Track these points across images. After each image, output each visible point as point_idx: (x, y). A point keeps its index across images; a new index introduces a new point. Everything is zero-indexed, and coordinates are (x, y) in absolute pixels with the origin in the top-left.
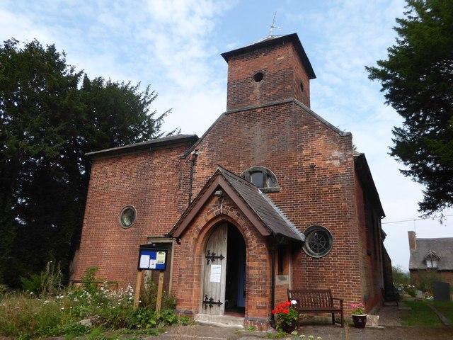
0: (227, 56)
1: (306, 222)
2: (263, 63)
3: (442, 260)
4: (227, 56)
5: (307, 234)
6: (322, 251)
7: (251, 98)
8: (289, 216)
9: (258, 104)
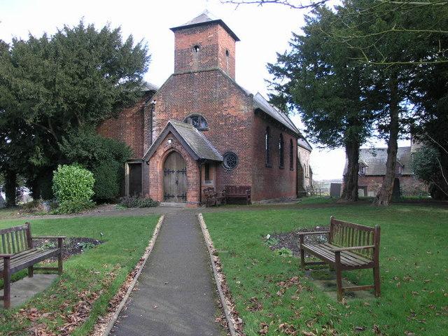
0: (174, 30)
1: (224, 149)
2: (199, 38)
3: (282, 171)
4: (174, 30)
5: (225, 156)
6: (7, 308)
7: (191, 64)
8: (214, 145)
9: (196, 70)
